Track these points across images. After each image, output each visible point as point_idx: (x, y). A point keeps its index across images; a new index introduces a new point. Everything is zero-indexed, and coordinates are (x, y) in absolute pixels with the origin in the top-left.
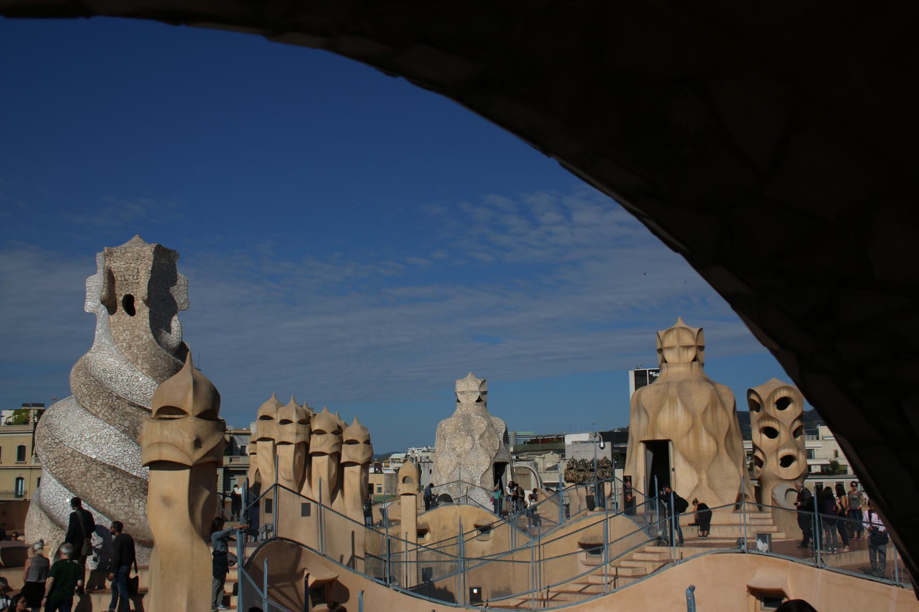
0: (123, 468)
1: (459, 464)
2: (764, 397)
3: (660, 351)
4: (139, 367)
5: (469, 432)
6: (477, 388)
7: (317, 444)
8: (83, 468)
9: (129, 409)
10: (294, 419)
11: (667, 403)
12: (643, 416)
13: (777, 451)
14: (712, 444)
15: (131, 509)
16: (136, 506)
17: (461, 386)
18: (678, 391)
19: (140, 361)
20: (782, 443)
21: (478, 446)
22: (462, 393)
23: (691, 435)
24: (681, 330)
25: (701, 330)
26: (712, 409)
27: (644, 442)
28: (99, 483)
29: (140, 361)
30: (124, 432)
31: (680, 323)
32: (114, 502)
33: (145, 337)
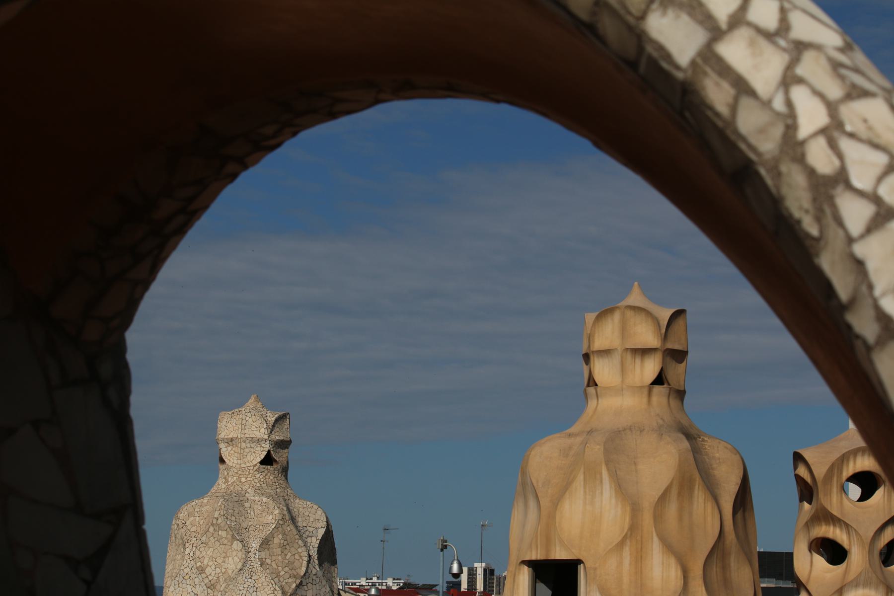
2: (820, 471)
3: (587, 357)
5: (238, 534)
6: (263, 433)
11: (581, 477)
12: (532, 504)
14: (674, 573)
17: (228, 426)
18: (607, 451)
20: (852, 576)
21: (257, 566)
22: (231, 441)
23: (627, 552)
24: (629, 313)
25: (678, 314)
26: (679, 494)
27: (530, 564)
31: (636, 298)
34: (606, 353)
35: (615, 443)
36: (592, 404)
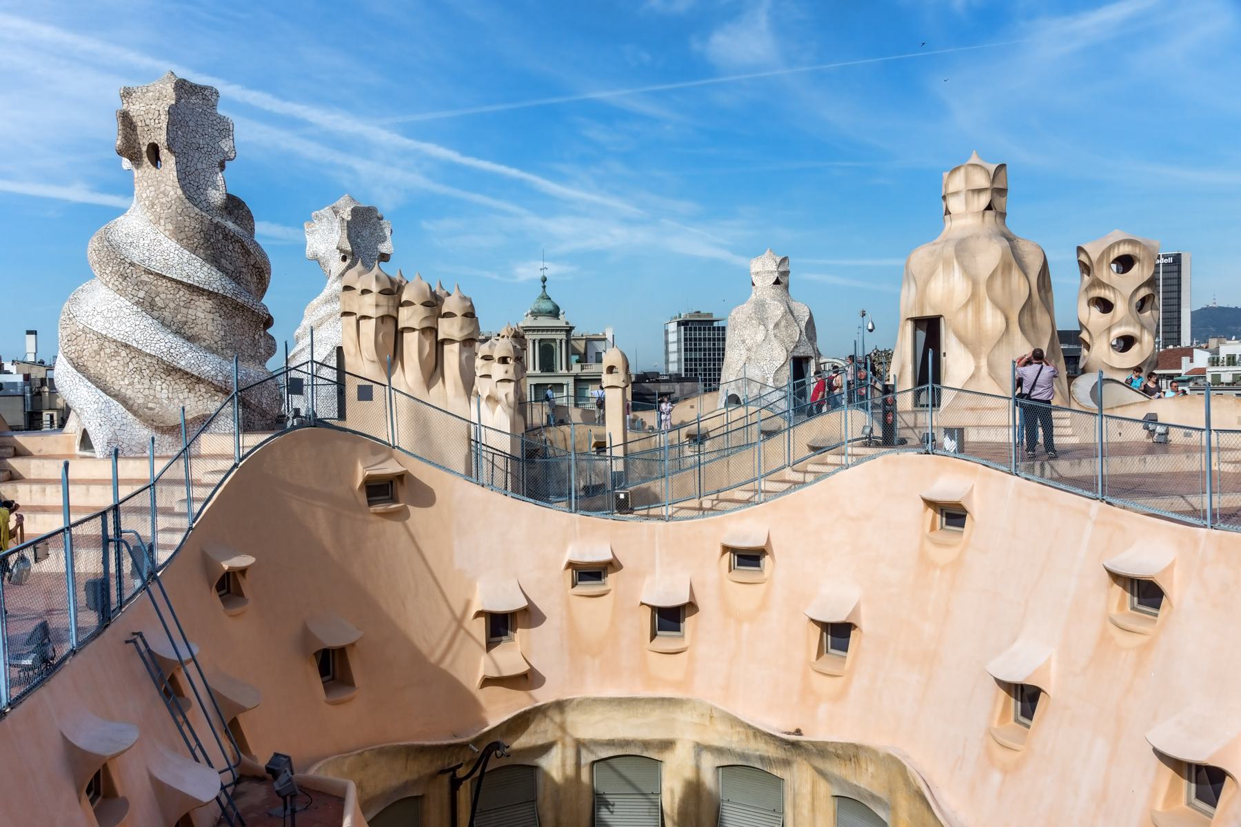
0: (135, 345)
1: (749, 358)
2: (1095, 256)
3: (944, 198)
4: (161, 228)
5: (762, 321)
6: (774, 268)
7: (407, 317)
8: (96, 347)
9: (145, 278)
10: (375, 288)
12: (912, 284)
13: (1109, 329)
14: (1000, 321)
15: (152, 392)
16: (158, 388)
19: (162, 222)
20: (1117, 319)
23: (970, 309)
24: (970, 168)
27: (911, 319)
28: (115, 363)
29: (162, 222)
30: (137, 303)
32: (132, 384)
33: (172, 193)
34: (956, 193)
35: (962, 248)
36: (948, 224)
